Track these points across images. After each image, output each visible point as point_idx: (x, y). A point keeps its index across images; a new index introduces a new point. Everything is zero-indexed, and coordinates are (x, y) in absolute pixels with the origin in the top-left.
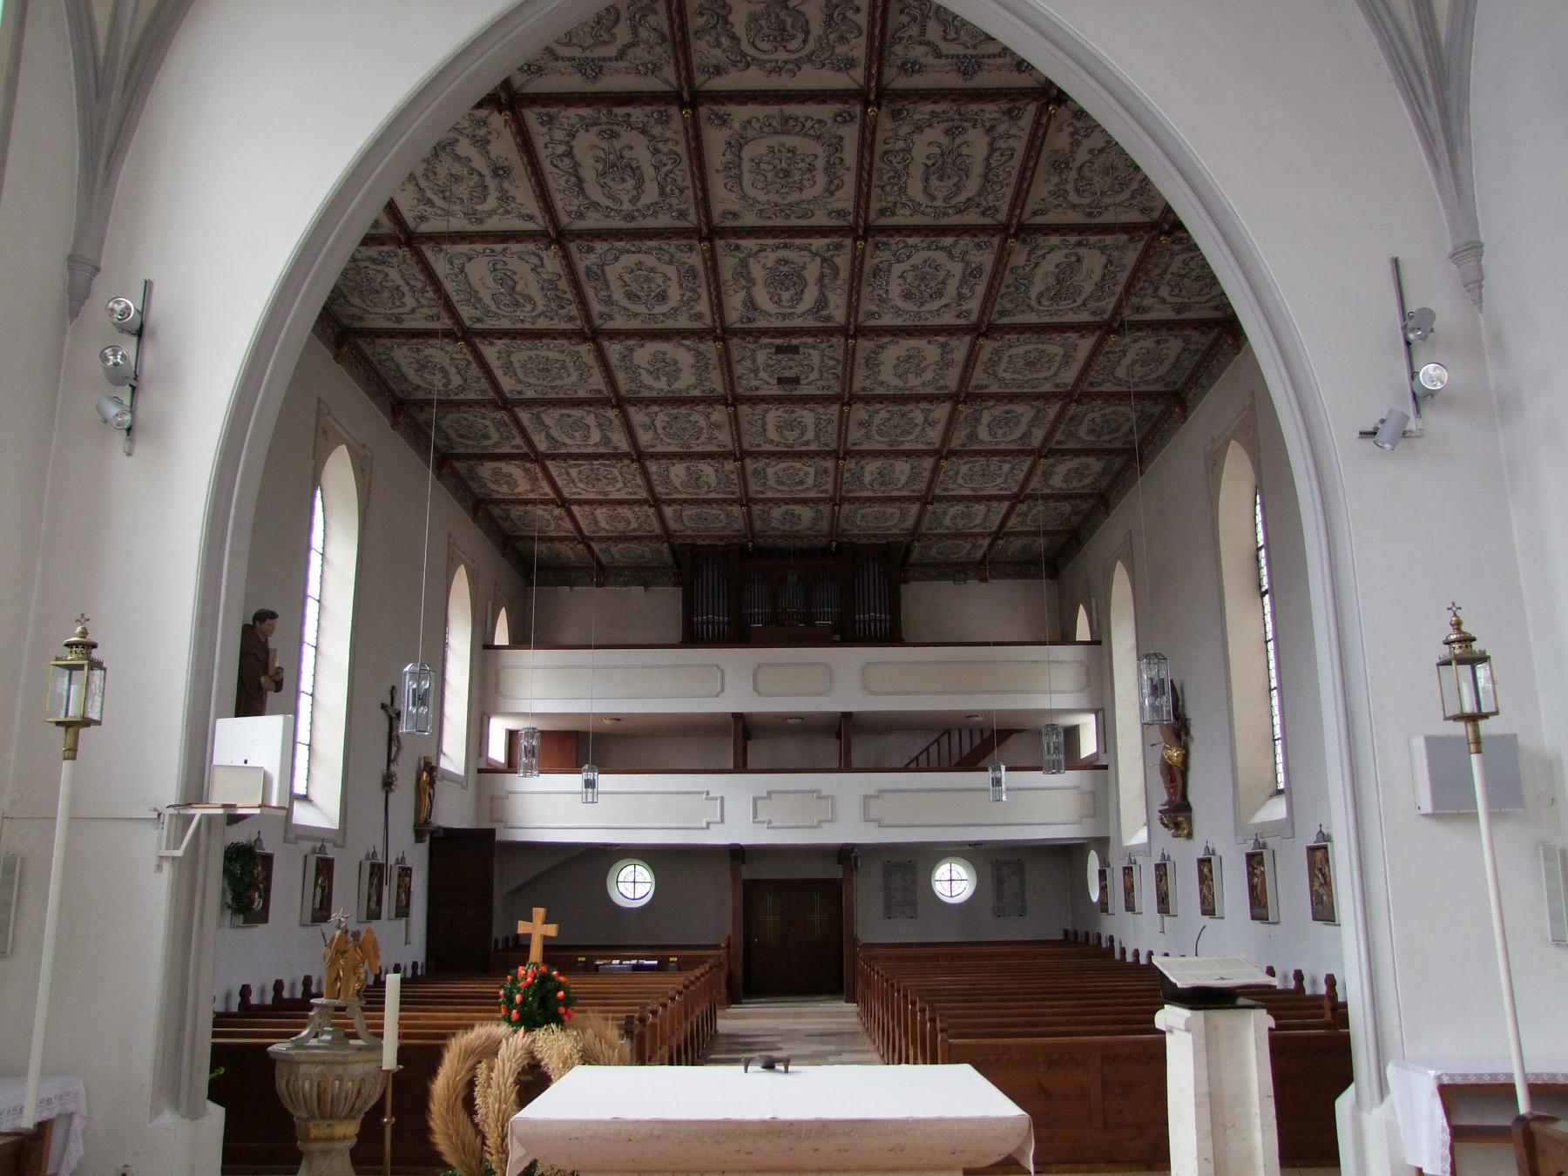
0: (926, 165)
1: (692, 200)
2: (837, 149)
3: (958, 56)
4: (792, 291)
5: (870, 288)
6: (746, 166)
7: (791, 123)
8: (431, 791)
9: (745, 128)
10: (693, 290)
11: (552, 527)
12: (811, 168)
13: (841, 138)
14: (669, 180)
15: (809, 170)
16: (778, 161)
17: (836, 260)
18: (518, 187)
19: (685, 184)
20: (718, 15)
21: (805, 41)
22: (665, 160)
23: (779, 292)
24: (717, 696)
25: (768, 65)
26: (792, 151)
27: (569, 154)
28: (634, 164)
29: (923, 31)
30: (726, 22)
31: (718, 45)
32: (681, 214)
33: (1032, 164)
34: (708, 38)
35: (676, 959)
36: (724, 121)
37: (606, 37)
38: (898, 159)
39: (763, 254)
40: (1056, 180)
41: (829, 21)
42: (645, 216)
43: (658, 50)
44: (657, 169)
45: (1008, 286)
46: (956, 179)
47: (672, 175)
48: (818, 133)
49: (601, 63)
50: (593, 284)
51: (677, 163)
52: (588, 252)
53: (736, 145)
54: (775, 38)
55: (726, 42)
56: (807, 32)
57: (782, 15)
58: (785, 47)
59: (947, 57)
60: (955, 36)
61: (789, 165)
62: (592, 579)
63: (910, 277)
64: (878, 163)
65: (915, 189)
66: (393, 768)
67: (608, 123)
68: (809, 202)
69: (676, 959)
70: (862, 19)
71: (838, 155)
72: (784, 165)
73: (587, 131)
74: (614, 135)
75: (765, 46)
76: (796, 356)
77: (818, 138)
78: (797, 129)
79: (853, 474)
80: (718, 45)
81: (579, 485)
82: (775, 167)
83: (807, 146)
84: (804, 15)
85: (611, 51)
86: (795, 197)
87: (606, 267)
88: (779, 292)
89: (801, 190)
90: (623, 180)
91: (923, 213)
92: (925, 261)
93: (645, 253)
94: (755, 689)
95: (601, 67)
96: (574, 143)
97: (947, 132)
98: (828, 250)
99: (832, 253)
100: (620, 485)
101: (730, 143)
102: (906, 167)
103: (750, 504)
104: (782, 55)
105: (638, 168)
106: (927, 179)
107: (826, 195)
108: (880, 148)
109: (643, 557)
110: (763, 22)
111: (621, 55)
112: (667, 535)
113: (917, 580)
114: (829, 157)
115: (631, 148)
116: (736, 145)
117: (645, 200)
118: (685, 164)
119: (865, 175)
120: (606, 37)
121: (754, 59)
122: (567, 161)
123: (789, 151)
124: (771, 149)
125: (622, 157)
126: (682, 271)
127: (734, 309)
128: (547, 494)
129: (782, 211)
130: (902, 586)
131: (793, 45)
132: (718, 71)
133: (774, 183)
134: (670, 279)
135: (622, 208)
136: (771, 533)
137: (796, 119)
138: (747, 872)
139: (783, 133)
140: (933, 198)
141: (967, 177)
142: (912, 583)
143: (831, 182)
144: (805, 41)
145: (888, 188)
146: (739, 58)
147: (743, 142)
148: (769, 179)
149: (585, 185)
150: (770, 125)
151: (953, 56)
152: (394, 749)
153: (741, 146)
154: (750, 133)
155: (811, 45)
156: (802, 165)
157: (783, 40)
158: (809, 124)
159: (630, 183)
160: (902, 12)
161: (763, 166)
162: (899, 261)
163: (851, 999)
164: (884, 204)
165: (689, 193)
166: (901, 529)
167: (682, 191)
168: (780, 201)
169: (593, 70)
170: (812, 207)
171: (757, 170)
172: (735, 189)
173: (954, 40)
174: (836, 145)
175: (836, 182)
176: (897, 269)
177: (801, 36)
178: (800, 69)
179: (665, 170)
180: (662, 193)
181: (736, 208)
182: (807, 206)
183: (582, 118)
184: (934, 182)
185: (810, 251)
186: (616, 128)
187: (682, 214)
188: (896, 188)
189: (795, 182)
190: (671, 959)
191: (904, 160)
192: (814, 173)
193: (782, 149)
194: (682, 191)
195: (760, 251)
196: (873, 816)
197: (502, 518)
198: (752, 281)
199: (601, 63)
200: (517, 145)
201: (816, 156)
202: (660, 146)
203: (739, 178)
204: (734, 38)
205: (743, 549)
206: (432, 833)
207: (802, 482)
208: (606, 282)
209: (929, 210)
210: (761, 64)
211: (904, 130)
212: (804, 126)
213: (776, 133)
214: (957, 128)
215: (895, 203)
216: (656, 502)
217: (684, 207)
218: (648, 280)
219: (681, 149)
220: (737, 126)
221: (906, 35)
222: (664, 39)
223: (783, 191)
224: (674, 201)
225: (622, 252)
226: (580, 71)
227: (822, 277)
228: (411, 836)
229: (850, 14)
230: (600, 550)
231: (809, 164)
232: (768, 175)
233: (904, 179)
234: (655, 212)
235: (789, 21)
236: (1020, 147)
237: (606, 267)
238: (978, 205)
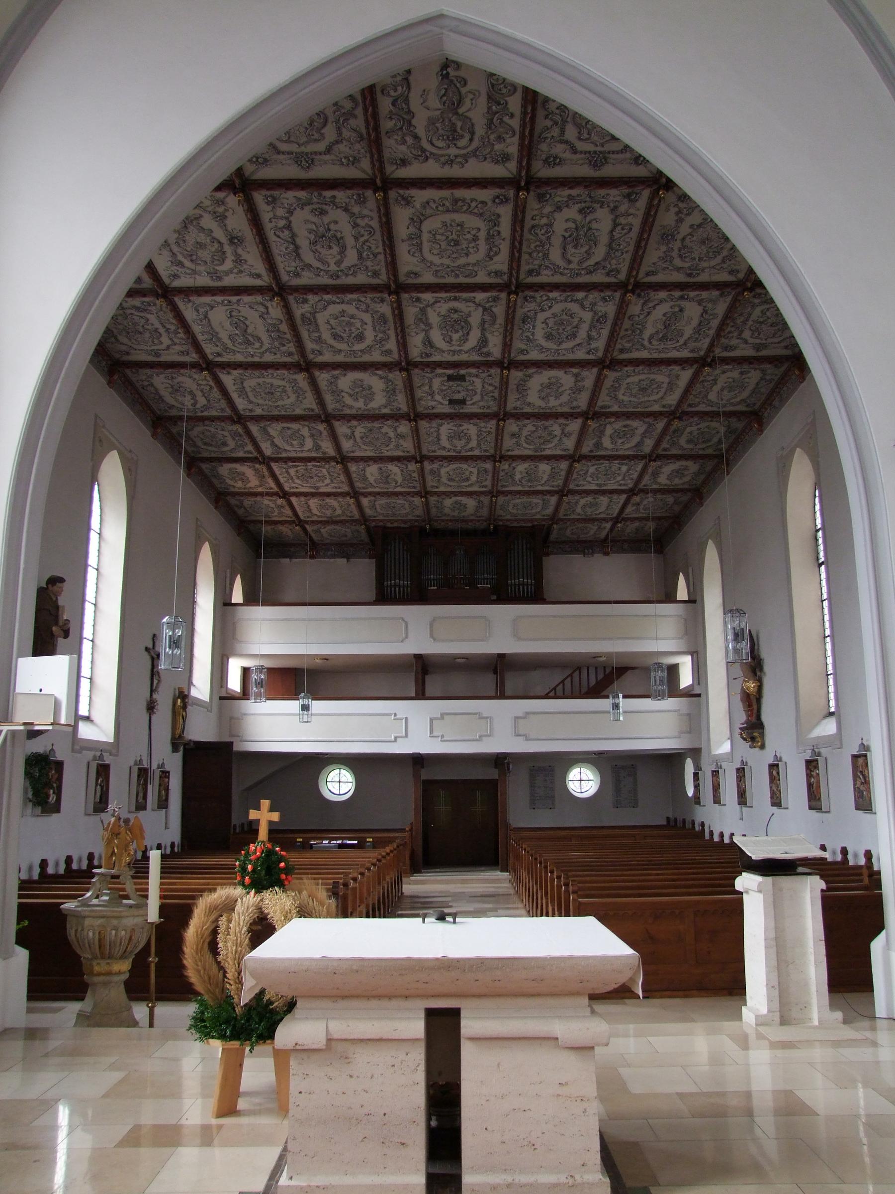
0: (564, 236)
1: (383, 263)
2: (495, 224)
3: (589, 152)
4: (461, 333)
5: (520, 331)
6: (425, 236)
7: (460, 203)
8: (184, 714)
9: (424, 207)
10: (384, 332)
11: (276, 514)
12: (475, 239)
13: (499, 216)
14: (366, 248)
15: (473, 240)
16: (449, 233)
17: (494, 309)
18: (249, 252)
19: (377, 251)
20: (403, 119)
21: (471, 140)
22: (362, 232)
23: (450, 333)
24: (402, 641)
25: (442, 159)
26: (461, 225)
27: (289, 227)
28: (339, 235)
29: (563, 132)
30: (410, 124)
31: (404, 142)
32: (375, 274)
33: (645, 236)
34: (396, 137)
35: (371, 840)
36: (408, 202)
37: (316, 136)
38: (543, 232)
39: (438, 304)
40: (664, 248)
41: (490, 125)
42: (347, 275)
43: (358, 146)
44: (356, 239)
45: (626, 330)
46: (587, 248)
47: (368, 244)
48: (481, 211)
49: (314, 156)
50: (307, 327)
51: (371, 233)
52: (303, 303)
53: (418, 221)
54: (448, 137)
55: (410, 140)
56: (473, 133)
57: (454, 119)
58: (455, 145)
59: (581, 152)
60: (588, 136)
61: (458, 236)
62: (307, 553)
63: (551, 322)
64: (526, 235)
65: (555, 255)
66: (155, 696)
67: (318, 203)
68: (474, 265)
69: (371, 840)
70: (515, 123)
71: (496, 228)
72: (454, 236)
74: (323, 212)
75: (440, 144)
76: (463, 383)
77: (481, 215)
78: (465, 208)
79: (506, 474)
80: (404, 142)
81: (297, 481)
83: (472, 222)
84: (470, 119)
85: (321, 147)
86: (462, 261)
87: (317, 315)
88: (450, 333)
89: (467, 255)
90: (330, 247)
91: (561, 274)
92: (563, 311)
93: (347, 303)
94: (432, 636)
95: (313, 160)
96: (291, 219)
98: (488, 302)
99: (492, 304)
100: (327, 481)
101: (412, 219)
102: (549, 238)
103: (428, 496)
104: (453, 151)
105: (342, 238)
106: (564, 248)
107: (487, 259)
108: (528, 223)
109: (346, 536)
110: (438, 125)
111: (329, 150)
112: (364, 519)
113: (556, 554)
114: (489, 230)
115: (336, 222)
116: (418, 221)
117: (347, 263)
118: (378, 235)
119: (517, 244)
120: (316, 136)
121: (431, 153)
122: (287, 232)
124: (445, 224)
125: (329, 230)
126: (376, 317)
127: (415, 346)
128: (271, 488)
129: (453, 271)
130: (544, 558)
131: (463, 143)
132: (404, 162)
133: (447, 250)
134: (366, 324)
136: (444, 518)
137: (464, 200)
138: (425, 775)
140: (570, 262)
141: (596, 245)
142: (552, 557)
143: (491, 249)
144: (471, 140)
145: (535, 255)
146: (420, 153)
147: (422, 218)
148: (443, 247)
149: (300, 251)
150: (444, 205)
151: (585, 153)
152: (155, 682)
153: (421, 222)
154: (428, 211)
155: (476, 143)
156: (469, 236)
157: (454, 139)
158: (474, 204)
159: (336, 249)
160: (546, 117)
161: (438, 237)
162: (543, 310)
163: (503, 870)
164: (531, 267)
165: (381, 257)
166: (544, 516)
167: (375, 255)
168: (452, 264)
169: (307, 162)
170: (476, 269)
171: (434, 241)
172: (416, 255)
174: (495, 221)
175: (494, 249)
176: (541, 317)
177: (467, 137)
178: (467, 162)
179: (362, 239)
180: (360, 257)
181: (417, 269)
183: (299, 199)
184: (570, 250)
185: (474, 302)
186: (324, 207)
187: (376, 274)
188: (540, 254)
189: (462, 249)
190: (368, 840)
191: (547, 232)
192: (477, 242)
193: (453, 224)
194: (375, 255)
195: (436, 302)
196: (521, 732)
197: (237, 506)
198: (429, 325)
199: (314, 156)
200: (248, 220)
201: (479, 230)
202: (359, 221)
204: (416, 137)
205: (422, 530)
206: (185, 745)
207: (467, 479)
208: (317, 325)
209: (566, 271)
210: (436, 157)
211: (548, 209)
212: (470, 206)
213: (448, 211)
216: (355, 494)
217: (377, 268)
218: (349, 324)
219: (375, 224)
220: (418, 206)
221: (549, 135)
223: (454, 256)
224: (369, 263)
225: (330, 303)
226: (297, 162)
227: (483, 322)
228: (169, 748)
229: (506, 119)
230: (313, 530)
231: (474, 236)
232: (442, 244)
233: (547, 247)
235: (459, 124)
236: (636, 222)
237: (317, 315)
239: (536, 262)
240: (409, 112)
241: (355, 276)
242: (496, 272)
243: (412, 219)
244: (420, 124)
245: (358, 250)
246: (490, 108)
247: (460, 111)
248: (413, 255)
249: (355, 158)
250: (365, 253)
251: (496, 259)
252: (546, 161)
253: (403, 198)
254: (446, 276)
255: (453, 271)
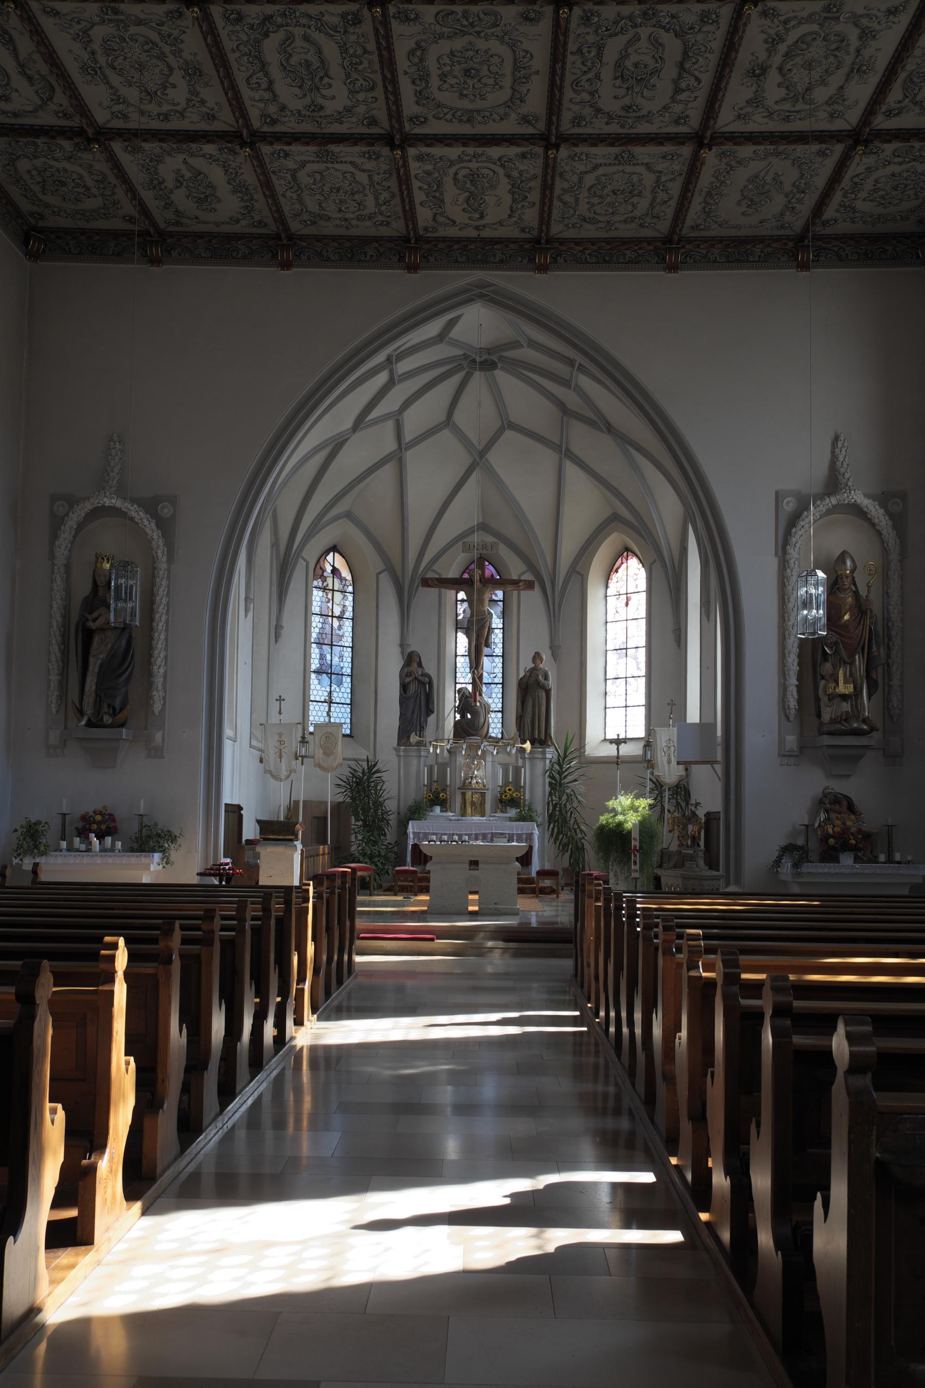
1: (572, 36)
2: (420, 94)
3: (337, 162)
6: (507, 82)
7: (465, 118)
9: (506, 114)
12: (443, 77)
13: (417, 103)
14: (589, 64)
15: (446, 76)
16: (476, 86)
18: (752, 54)
20: (519, 188)
21: (456, 174)
22: (587, 86)
25: (484, 159)
26: (462, 96)
27: (678, 90)
29: (370, 177)
30: (513, 185)
31: (521, 173)
32: (588, 19)
34: (528, 176)
36: (525, 119)
37: (603, 179)
38: (358, 84)
41: (440, 184)
42: (630, 17)
43: (567, 168)
44: (598, 77)
46: (293, 61)
47: (585, 69)
48: (439, 110)
51: (577, 82)
53: (516, 99)
54: (478, 176)
55: (515, 174)
56: (455, 179)
57: (473, 189)
58: (471, 171)
59: (346, 162)
60: (346, 175)
61: (465, 83)
64: (378, 78)
65: (331, 50)
67: (628, 118)
68: (441, 36)
70: (416, 184)
71: (419, 89)
73: (649, 112)
74: (627, 108)
75: (486, 171)
77: (439, 105)
78: (459, 113)
80: (521, 173)
82: (479, 81)
83: (448, 98)
84: (458, 188)
85: (601, 170)
86: (458, 44)
89: (452, 53)
90: (636, 65)
91: (310, 17)
97: (321, 108)
101: (521, 101)
102: (348, 76)
104: (474, 165)
105: (616, 78)
106: (322, 62)
107: (423, 44)
108: (379, 92)
110: (487, 185)
111: (596, 167)
114: (427, 87)
116: (516, 99)
117: (622, 40)
118: (569, 78)
119: (390, 89)
120: (603, 179)
121: (495, 164)
122: (683, 85)
123: (466, 96)
124: (483, 97)
125: (628, 89)
129: (472, 25)
131: (464, 172)
132: (524, 156)
135: (651, 29)
137: (460, 121)
139: (472, 111)
140: (306, 38)
141: (282, 64)
143: (421, 60)
146: (507, 164)
147: (509, 104)
148: (485, 67)
150: (483, 117)
151: (341, 162)
153: (511, 99)
154: (502, 111)
155: (452, 170)
156: (452, 81)
157: (473, 175)
158: (449, 117)
160: (389, 187)
161: (491, 81)
165: (572, 47)
168: (471, 38)
169: (622, 157)
170: (438, 28)
172: (522, 54)
173: (346, 173)
174: (421, 97)
175: (416, 60)
177: (459, 176)
178: (459, 156)
179: (590, 75)
180: (600, 49)
182: (445, 30)
184: (312, 57)
186: (623, 113)
188: (351, 51)
192: (440, 72)
193: (472, 98)
194: (580, 51)
200: (737, 52)
202: (586, 97)
203: (516, 67)
204: (509, 176)
211: (361, 109)
212: (453, 115)
213: (478, 111)
214: (314, 111)
215: (346, 32)
217: (582, 30)
219: (568, 93)
220: (513, 116)
221: (381, 176)
222: (561, 175)
223: (471, 53)
224: (591, 38)
226: (633, 156)
229: (425, 187)
231: (445, 81)
232: (487, 73)
233: (346, 63)
234: (616, 23)
235: (468, 185)
238: (252, 27)
239: (353, 38)
240: (513, 194)
241: (618, 14)
242: (408, 19)
243: (521, 101)
244: (504, 185)
245: (601, 61)
246: (442, 194)
247: (467, 194)
248: (527, 52)
249: (573, 159)
250: (592, 55)
251: (411, 44)
252: (378, 156)
253: (529, 122)
254: (481, 15)
255: (472, 25)
